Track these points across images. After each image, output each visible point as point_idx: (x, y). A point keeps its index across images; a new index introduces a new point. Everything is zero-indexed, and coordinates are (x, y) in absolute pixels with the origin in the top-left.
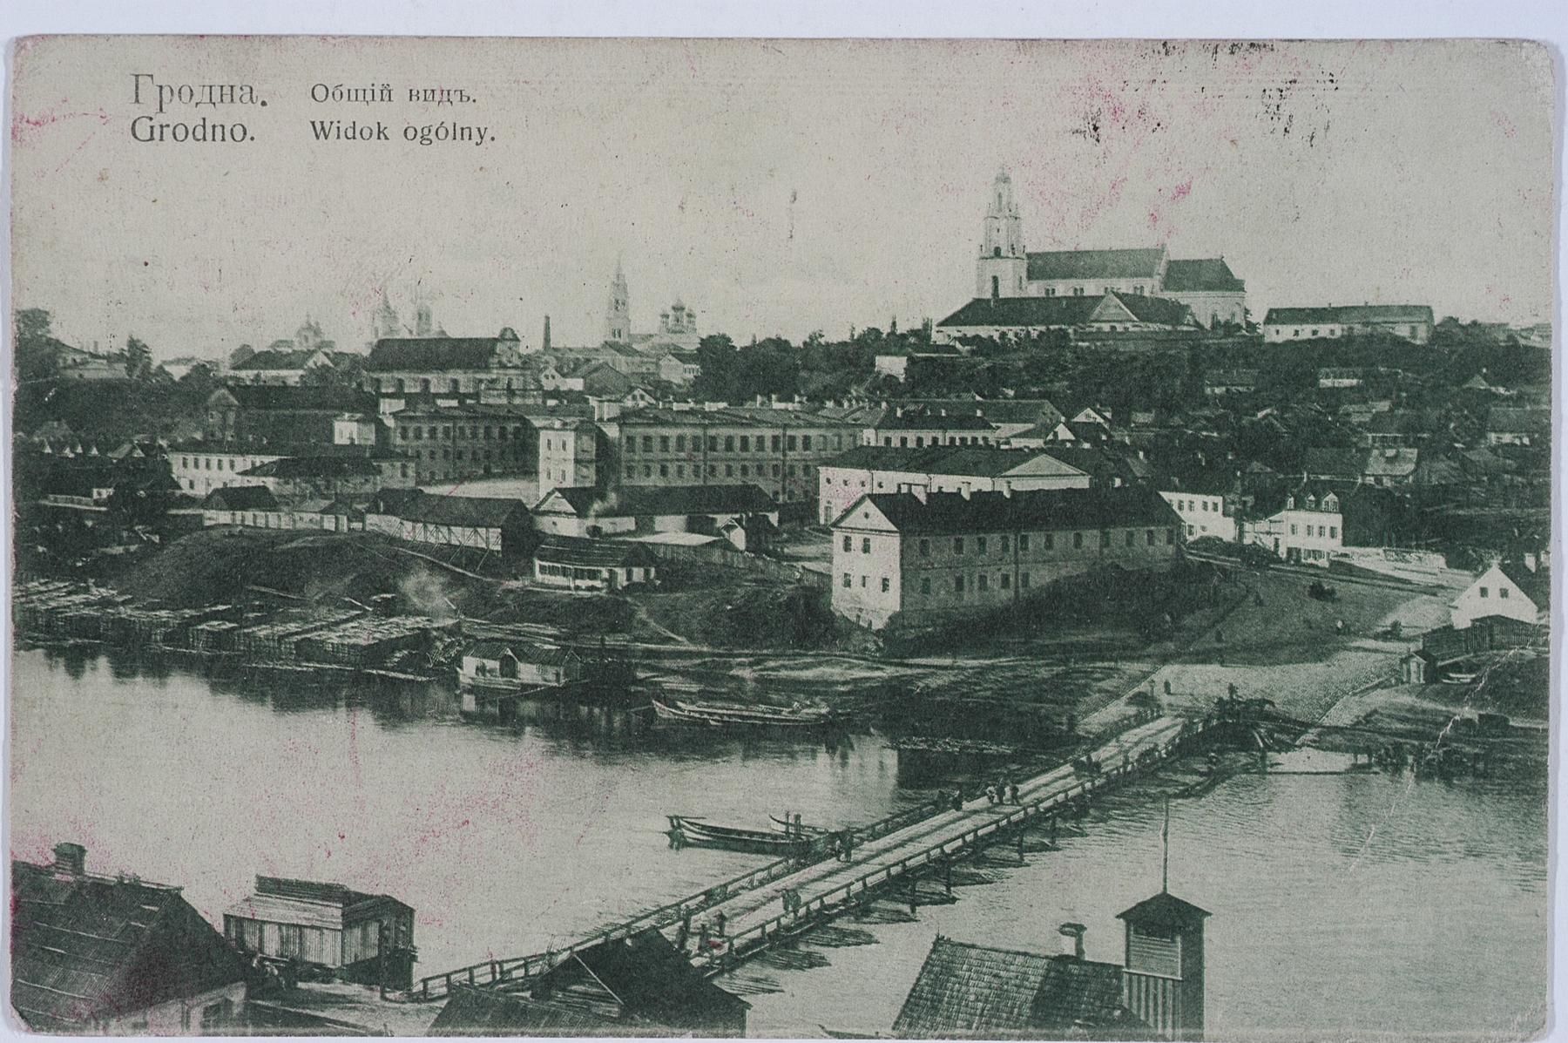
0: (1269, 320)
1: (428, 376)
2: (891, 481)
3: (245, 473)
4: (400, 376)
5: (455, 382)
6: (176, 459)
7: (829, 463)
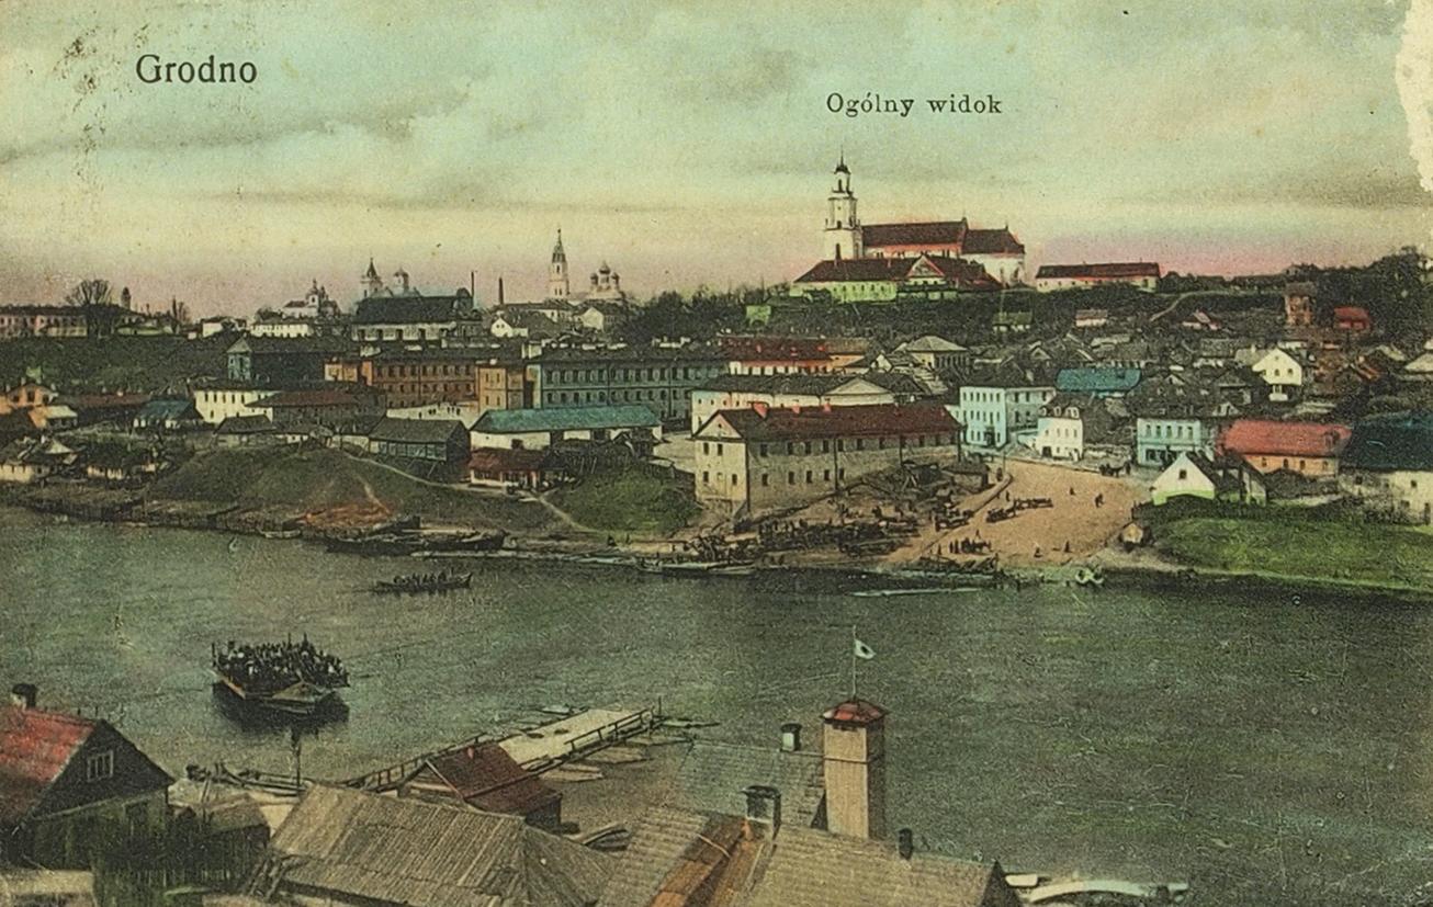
0: (1039, 276)
1: (403, 327)
2: (742, 400)
3: (253, 405)
4: (362, 327)
5: (423, 332)
6: (199, 395)
7: (705, 388)
